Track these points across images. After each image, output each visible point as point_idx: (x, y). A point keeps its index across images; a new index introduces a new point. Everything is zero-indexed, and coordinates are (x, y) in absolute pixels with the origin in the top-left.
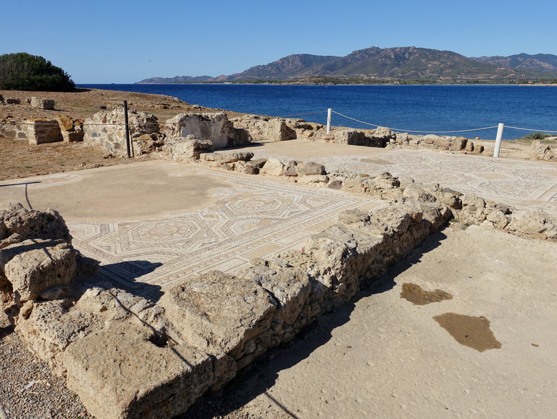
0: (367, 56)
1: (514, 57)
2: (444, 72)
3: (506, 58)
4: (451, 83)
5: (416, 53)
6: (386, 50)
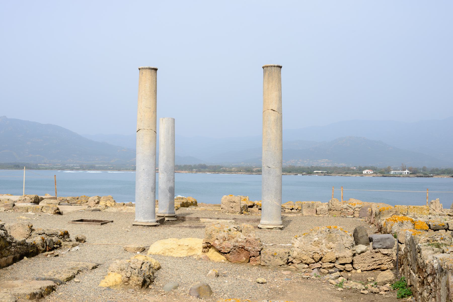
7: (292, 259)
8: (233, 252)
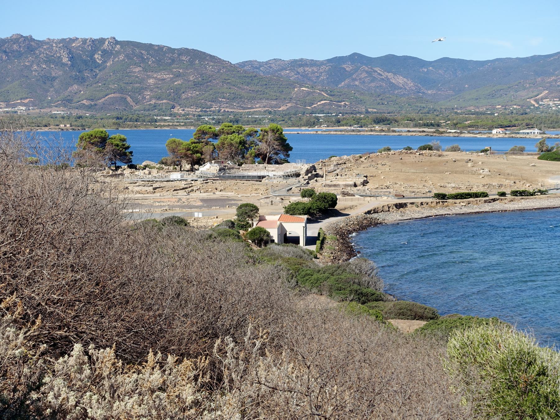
0: (4, 57)
1: (337, 61)
2: (184, 96)
3: (322, 63)
5: (118, 53)
6: (49, 42)
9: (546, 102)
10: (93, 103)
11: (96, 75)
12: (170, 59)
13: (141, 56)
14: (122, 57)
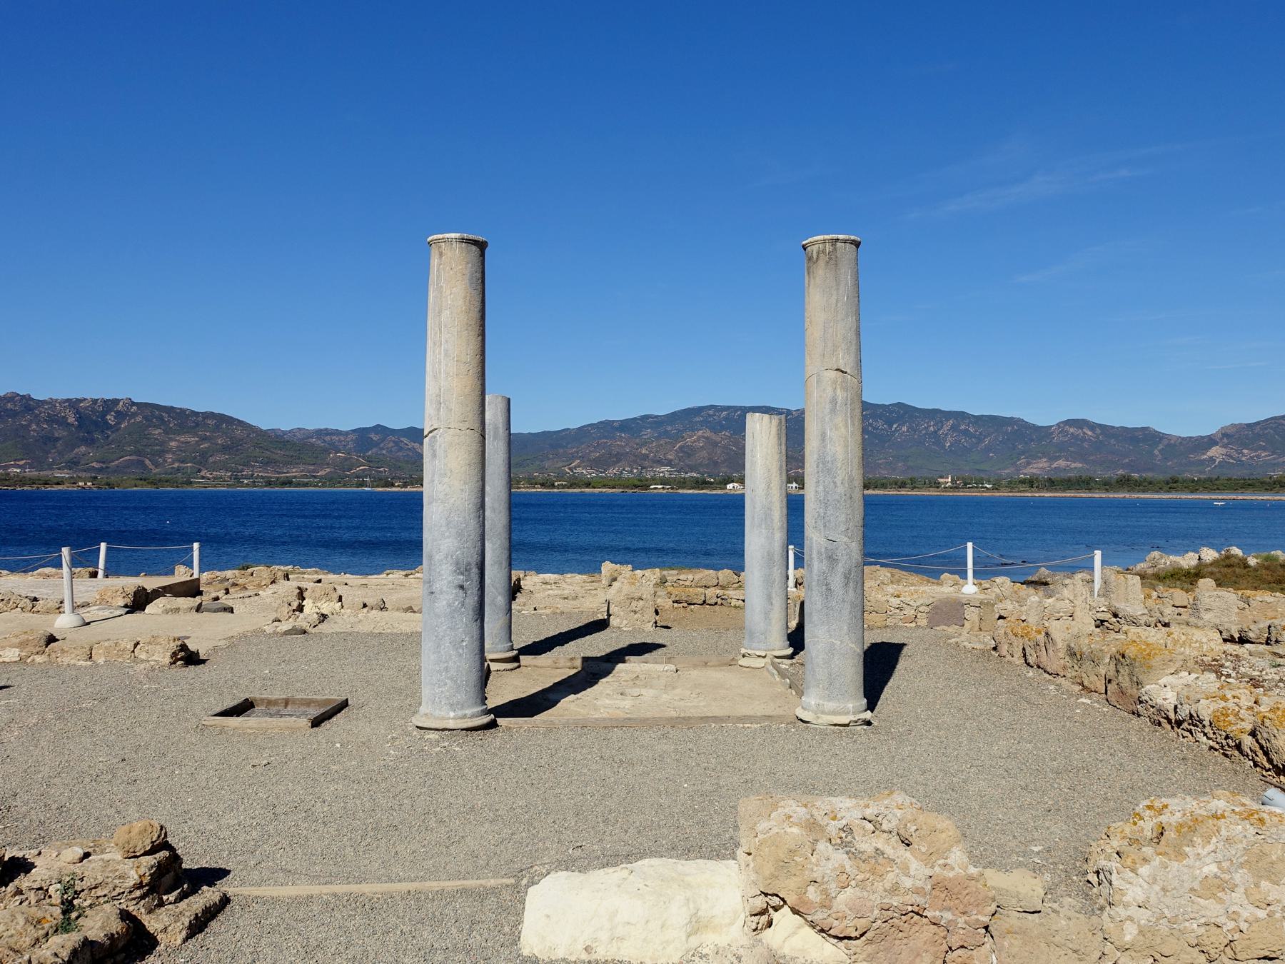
2: (211, 460)
4: (229, 486)
5: (135, 414)
7: (1119, 954)
8: (878, 931)
9: (579, 470)
10: (104, 466)
11: (108, 437)
12: (194, 422)
13: (161, 418)
14: (139, 419)
